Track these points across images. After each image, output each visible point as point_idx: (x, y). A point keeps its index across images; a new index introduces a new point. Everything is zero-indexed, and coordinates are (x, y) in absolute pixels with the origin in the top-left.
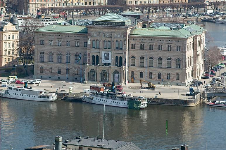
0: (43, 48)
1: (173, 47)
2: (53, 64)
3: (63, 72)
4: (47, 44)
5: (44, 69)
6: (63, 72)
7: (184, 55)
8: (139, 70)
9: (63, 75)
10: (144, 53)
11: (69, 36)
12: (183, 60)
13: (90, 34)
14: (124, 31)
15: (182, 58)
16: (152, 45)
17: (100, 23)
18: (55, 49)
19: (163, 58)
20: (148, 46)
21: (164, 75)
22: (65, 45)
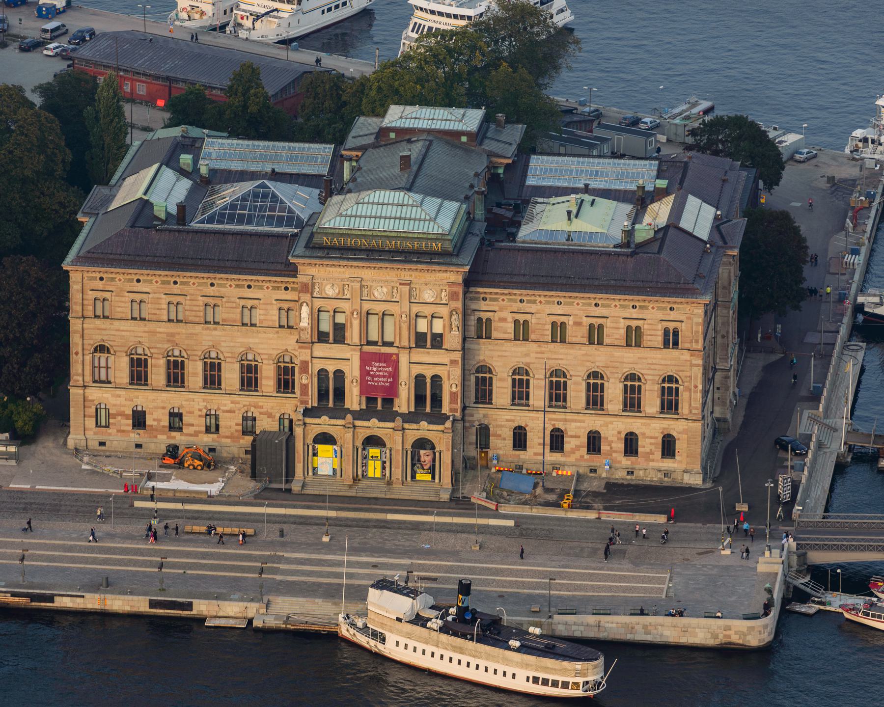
0: (105, 330)
1: (649, 332)
3: (192, 425)
4: (123, 316)
6: (192, 425)
7: (694, 362)
8: (508, 420)
9: (191, 435)
10: (527, 355)
11: (212, 285)
12: (690, 382)
13: (308, 288)
15: (688, 374)
16: (563, 324)
19: (607, 373)
22: (197, 320)
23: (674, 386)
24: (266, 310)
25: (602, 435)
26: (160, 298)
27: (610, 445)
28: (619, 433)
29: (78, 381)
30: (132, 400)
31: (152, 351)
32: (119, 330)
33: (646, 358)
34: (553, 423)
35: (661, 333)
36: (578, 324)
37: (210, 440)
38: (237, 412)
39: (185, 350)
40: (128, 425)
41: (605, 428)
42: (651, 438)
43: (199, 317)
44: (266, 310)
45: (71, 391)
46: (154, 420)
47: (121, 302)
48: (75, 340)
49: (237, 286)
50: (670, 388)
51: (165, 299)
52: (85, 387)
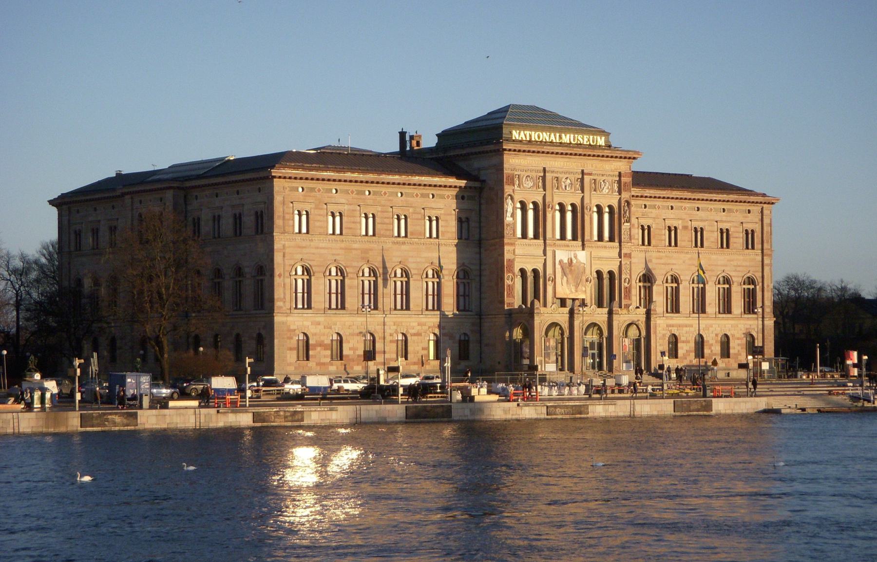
2: (347, 319)
5: (311, 342)
14: (622, 166)
17: (530, 136)
18: (354, 252)
20: (664, 231)
21: (711, 342)
22: (388, 233)
23: (751, 287)
24: (446, 221)
25: (705, 339)
26: (355, 210)
27: (710, 348)
28: (717, 335)
29: (282, 307)
30: (331, 328)
32: (317, 248)
33: (732, 260)
34: (670, 328)
35: (742, 235)
36: (685, 228)
38: (423, 334)
39: (377, 267)
40: (325, 356)
41: (706, 332)
42: (738, 339)
44: (446, 221)
45: (275, 318)
46: (350, 349)
47: (320, 215)
48: (278, 258)
49: (423, 196)
50: (749, 289)
52: (288, 315)
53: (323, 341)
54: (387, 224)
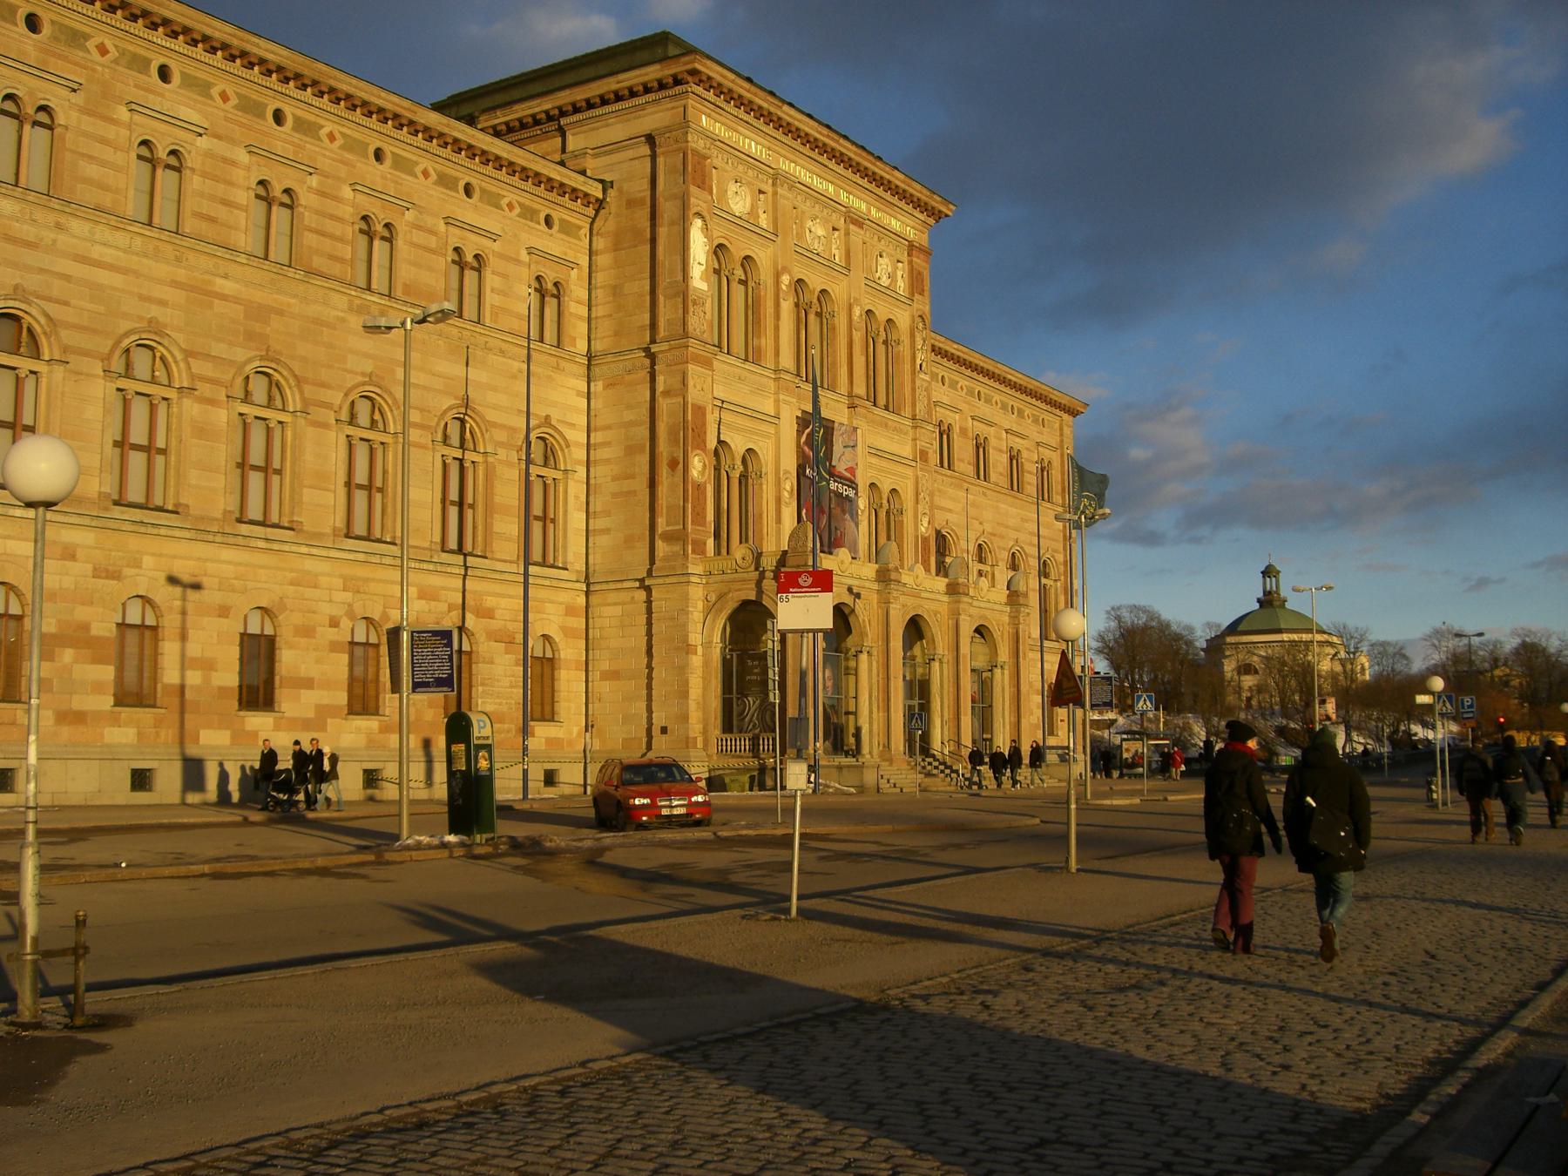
3: (308, 683)
4: (107, 200)
6: (308, 683)
24: (504, 276)
26: (233, 163)
30: (115, 575)
31: (198, 367)
37: (361, 741)
39: (295, 376)
40: (98, 688)
43: (341, 260)
47: (104, 141)
51: (247, 170)
53: (85, 627)
54: (332, 237)
